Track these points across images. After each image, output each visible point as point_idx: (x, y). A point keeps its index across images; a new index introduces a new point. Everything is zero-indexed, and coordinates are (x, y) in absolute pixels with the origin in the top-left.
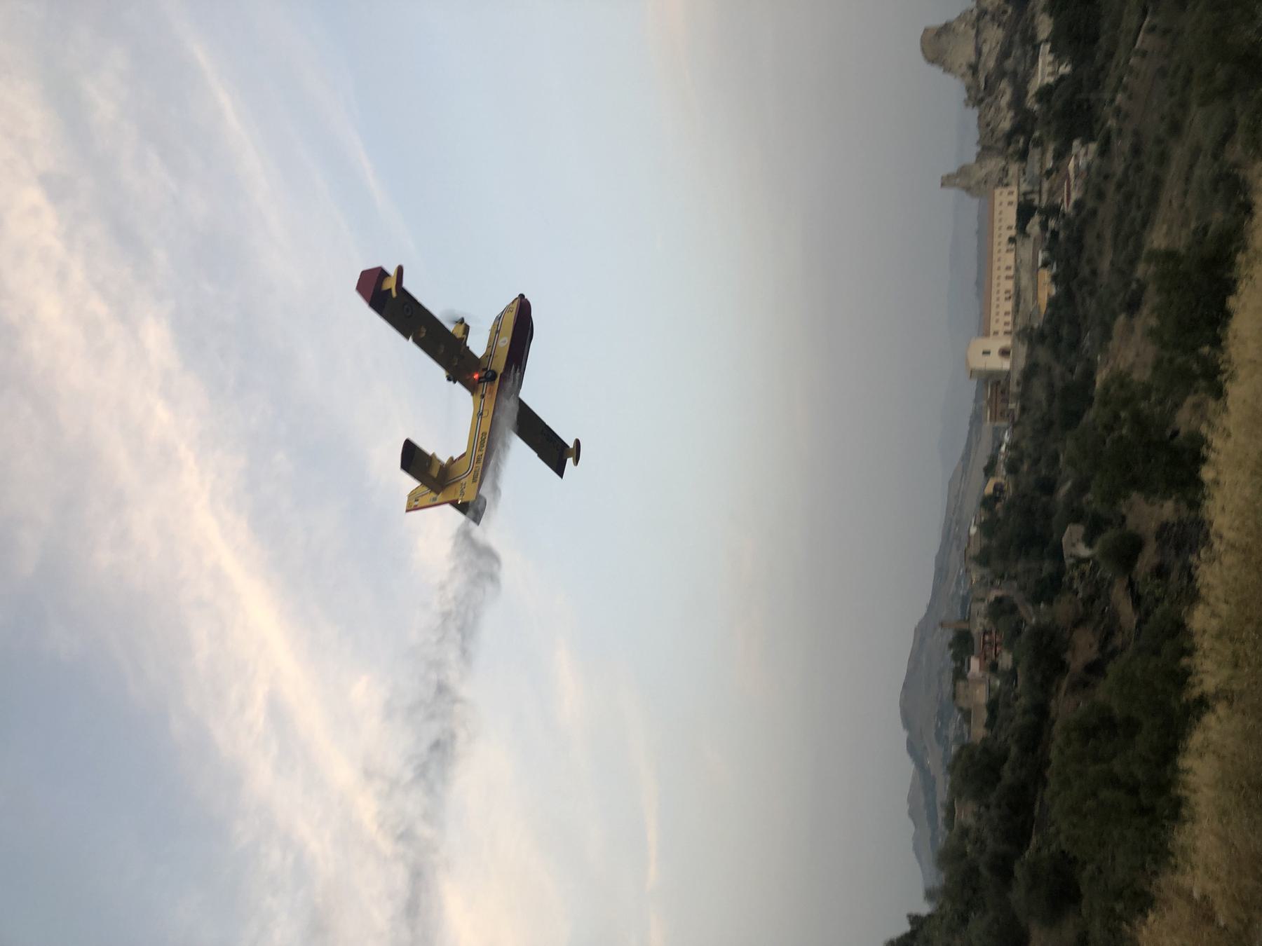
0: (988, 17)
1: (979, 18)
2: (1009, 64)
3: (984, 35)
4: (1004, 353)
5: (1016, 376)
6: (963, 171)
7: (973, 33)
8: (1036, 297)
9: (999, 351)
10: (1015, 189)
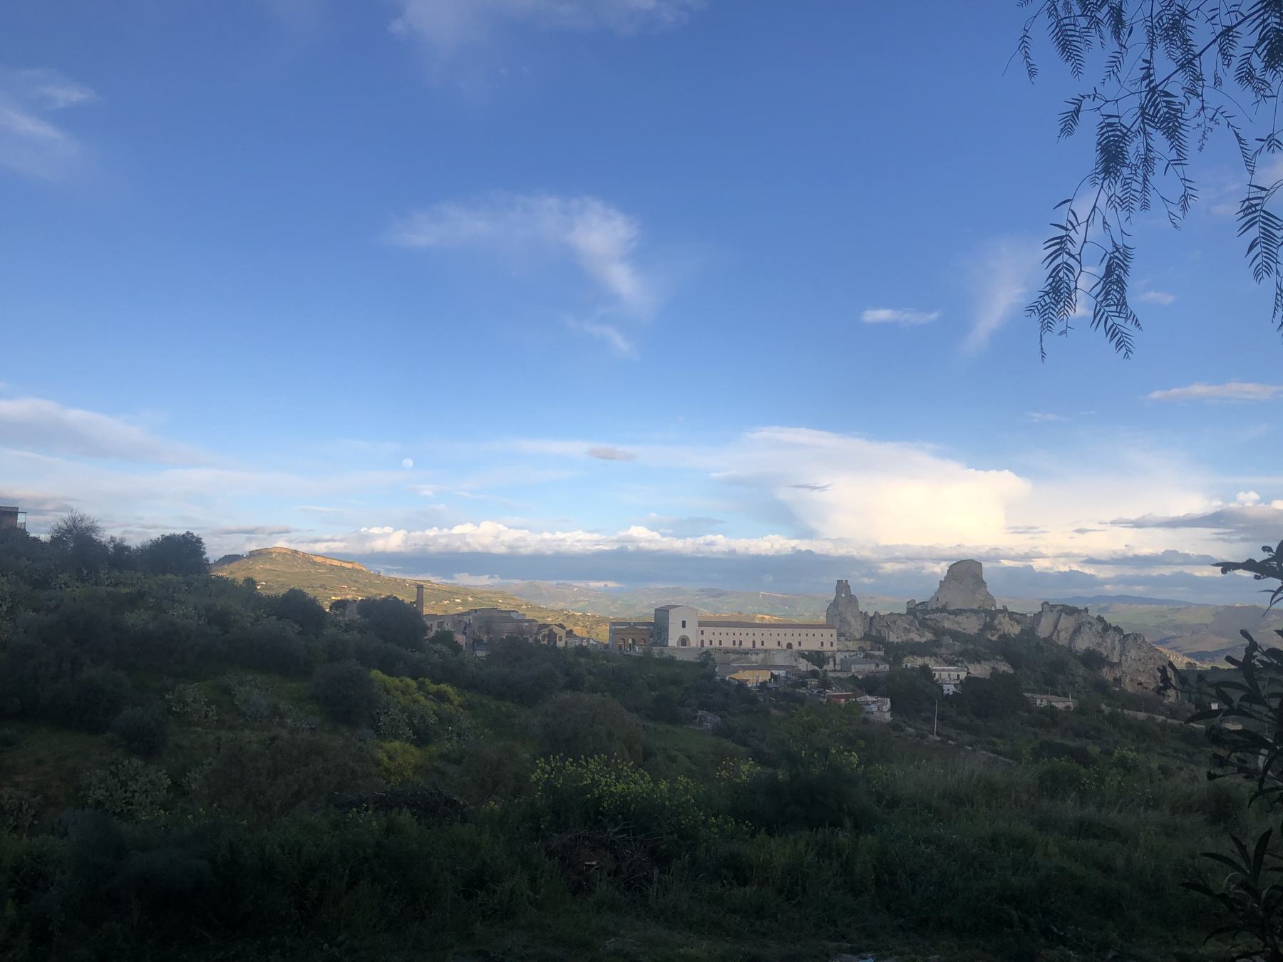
1: (986, 611)
2: (947, 640)
3: (974, 618)
4: (684, 641)
5: (667, 653)
6: (852, 600)
7: (975, 607)
8: (745, 668)
9: (688, 638)
10: (835, 648)
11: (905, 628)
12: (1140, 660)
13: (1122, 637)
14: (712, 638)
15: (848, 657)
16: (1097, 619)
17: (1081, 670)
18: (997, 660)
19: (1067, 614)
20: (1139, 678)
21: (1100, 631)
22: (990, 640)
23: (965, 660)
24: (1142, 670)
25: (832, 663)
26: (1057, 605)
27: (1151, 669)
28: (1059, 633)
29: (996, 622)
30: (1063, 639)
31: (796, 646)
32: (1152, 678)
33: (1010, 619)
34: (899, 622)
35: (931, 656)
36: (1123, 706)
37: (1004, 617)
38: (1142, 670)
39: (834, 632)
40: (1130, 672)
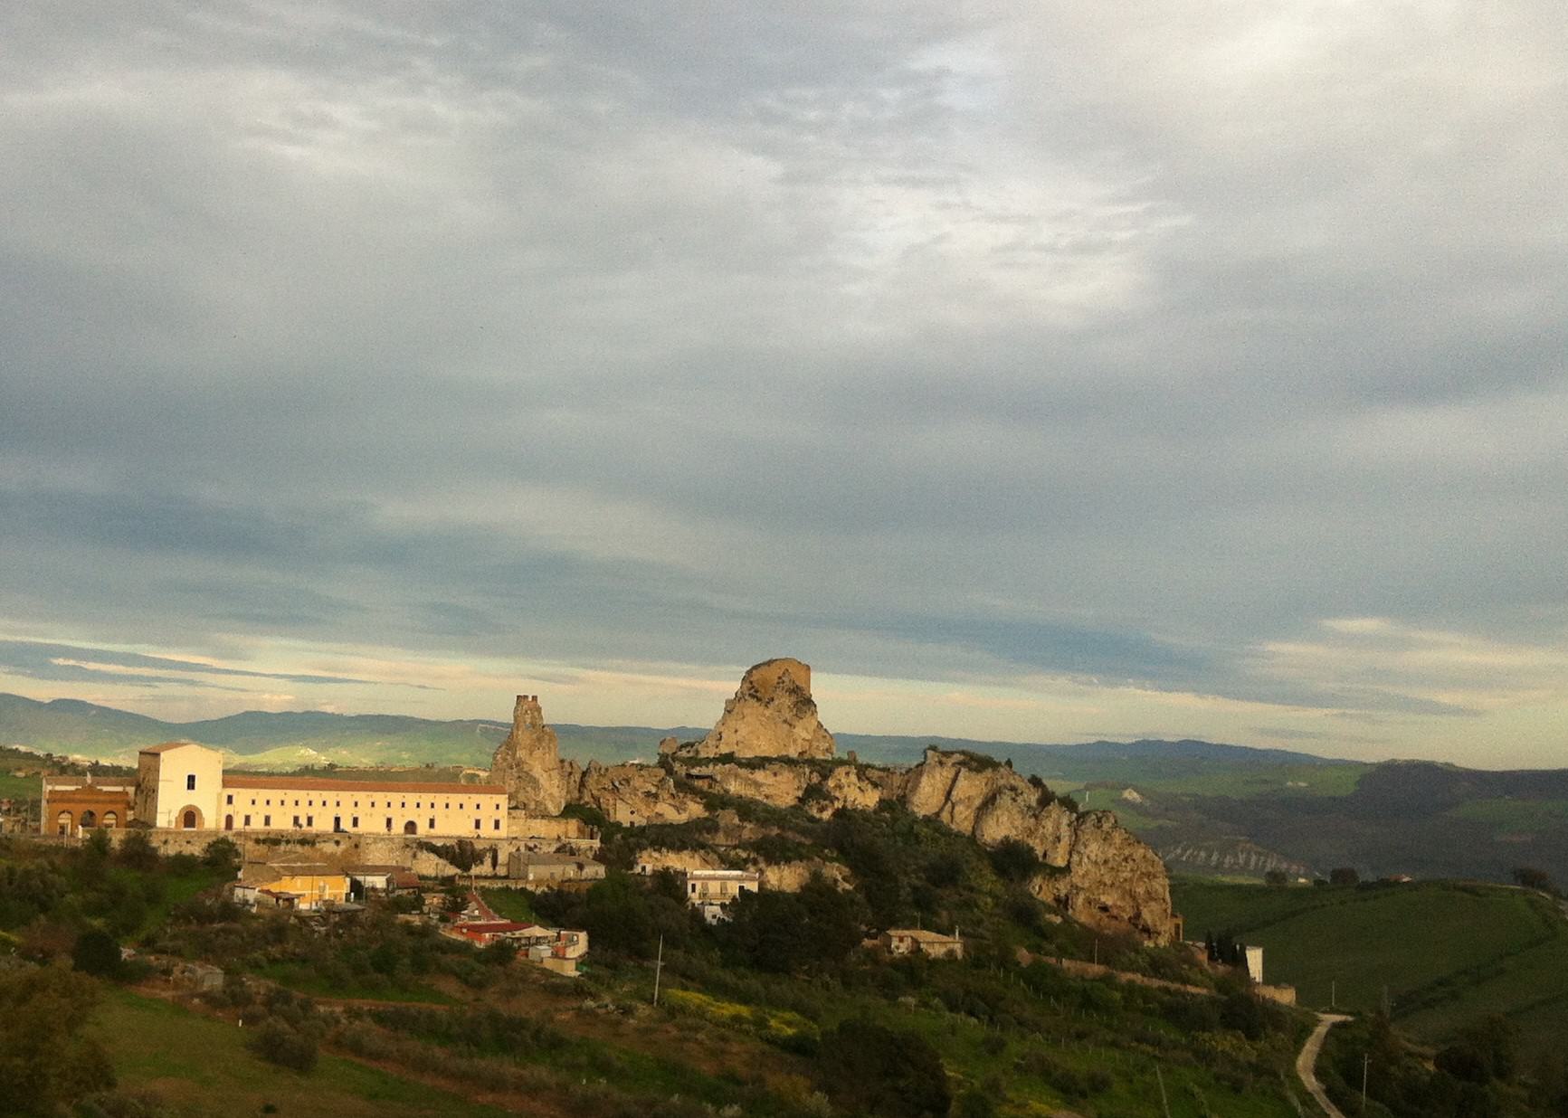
0: (815, 779)
1: (812, 762)
2: (729, 818)
4: (190, 817)
7: (793, 754)
9: (199, 811)
10: (503, 832)
11: (648, 794)
12: (1106, 862)
13: (1075, 815)
14: (249, 810)
15: (522, 849)
16: (1030, 781)
17: (988, 881)
18: (825, 859)
19: (970, 770)
20: (1103, 899)
21: (1034, 804)
22: (812, 819)
23: (761, 859)
24: (1109, 882)
25: (488, 861)
26: (952, 753)
27: (1126, 880)
28: (953, 808)
29: (831, 783)
30: (962, 820)
31: (423, 830)
32: (1127, 897)
33: (859, 779)
34: (637, 782)
35: (694, 850)
36: (1062, 952)
37: (847, 774)
38: (1109, 882)
39: (503, 800)
40: (1086, 885)
